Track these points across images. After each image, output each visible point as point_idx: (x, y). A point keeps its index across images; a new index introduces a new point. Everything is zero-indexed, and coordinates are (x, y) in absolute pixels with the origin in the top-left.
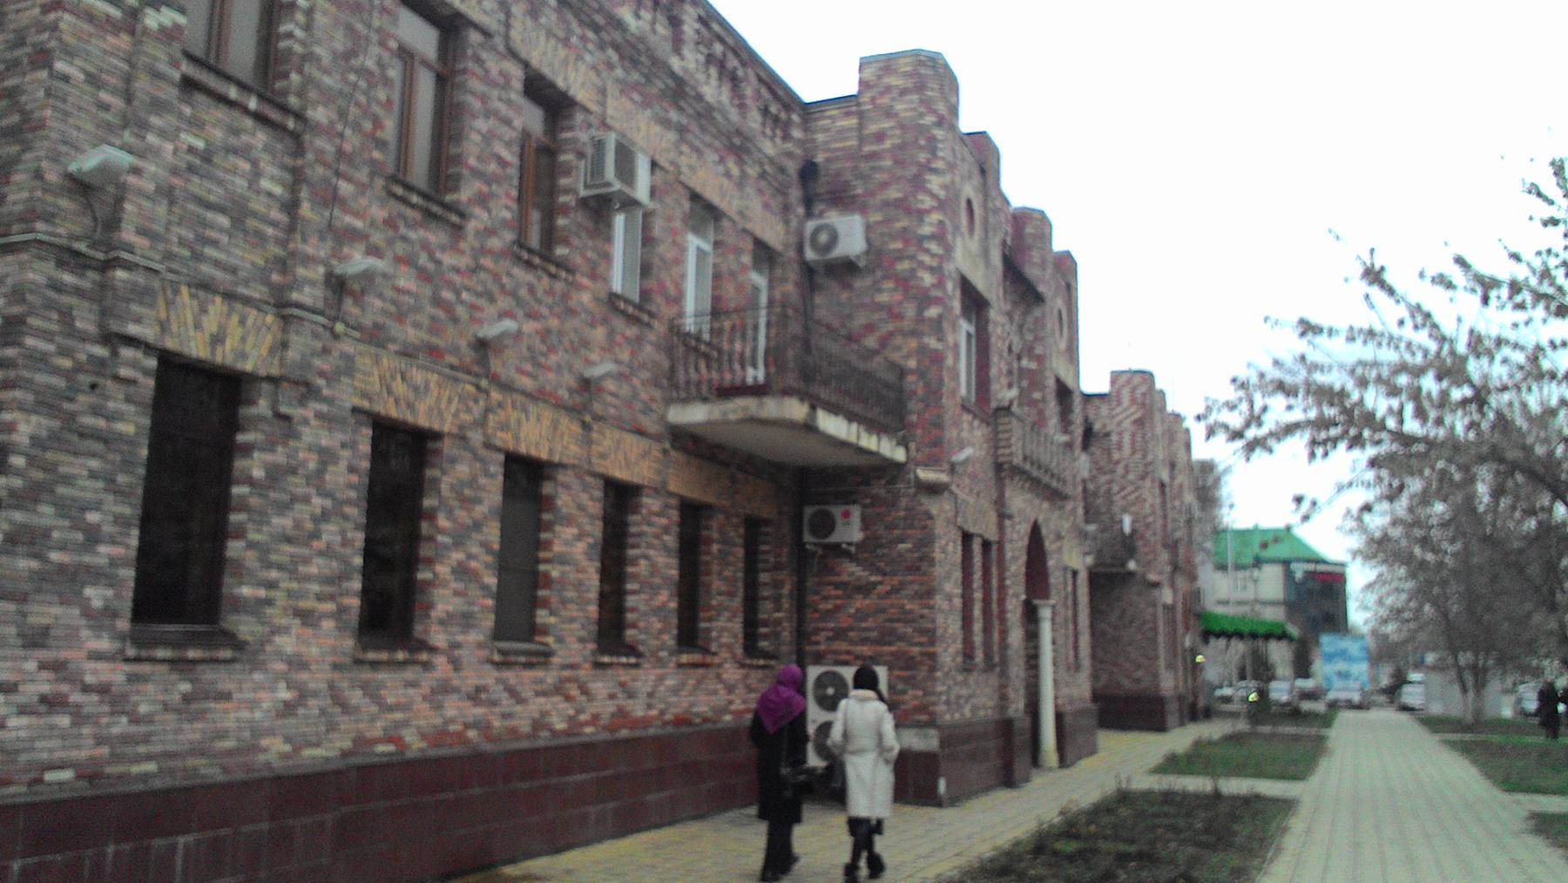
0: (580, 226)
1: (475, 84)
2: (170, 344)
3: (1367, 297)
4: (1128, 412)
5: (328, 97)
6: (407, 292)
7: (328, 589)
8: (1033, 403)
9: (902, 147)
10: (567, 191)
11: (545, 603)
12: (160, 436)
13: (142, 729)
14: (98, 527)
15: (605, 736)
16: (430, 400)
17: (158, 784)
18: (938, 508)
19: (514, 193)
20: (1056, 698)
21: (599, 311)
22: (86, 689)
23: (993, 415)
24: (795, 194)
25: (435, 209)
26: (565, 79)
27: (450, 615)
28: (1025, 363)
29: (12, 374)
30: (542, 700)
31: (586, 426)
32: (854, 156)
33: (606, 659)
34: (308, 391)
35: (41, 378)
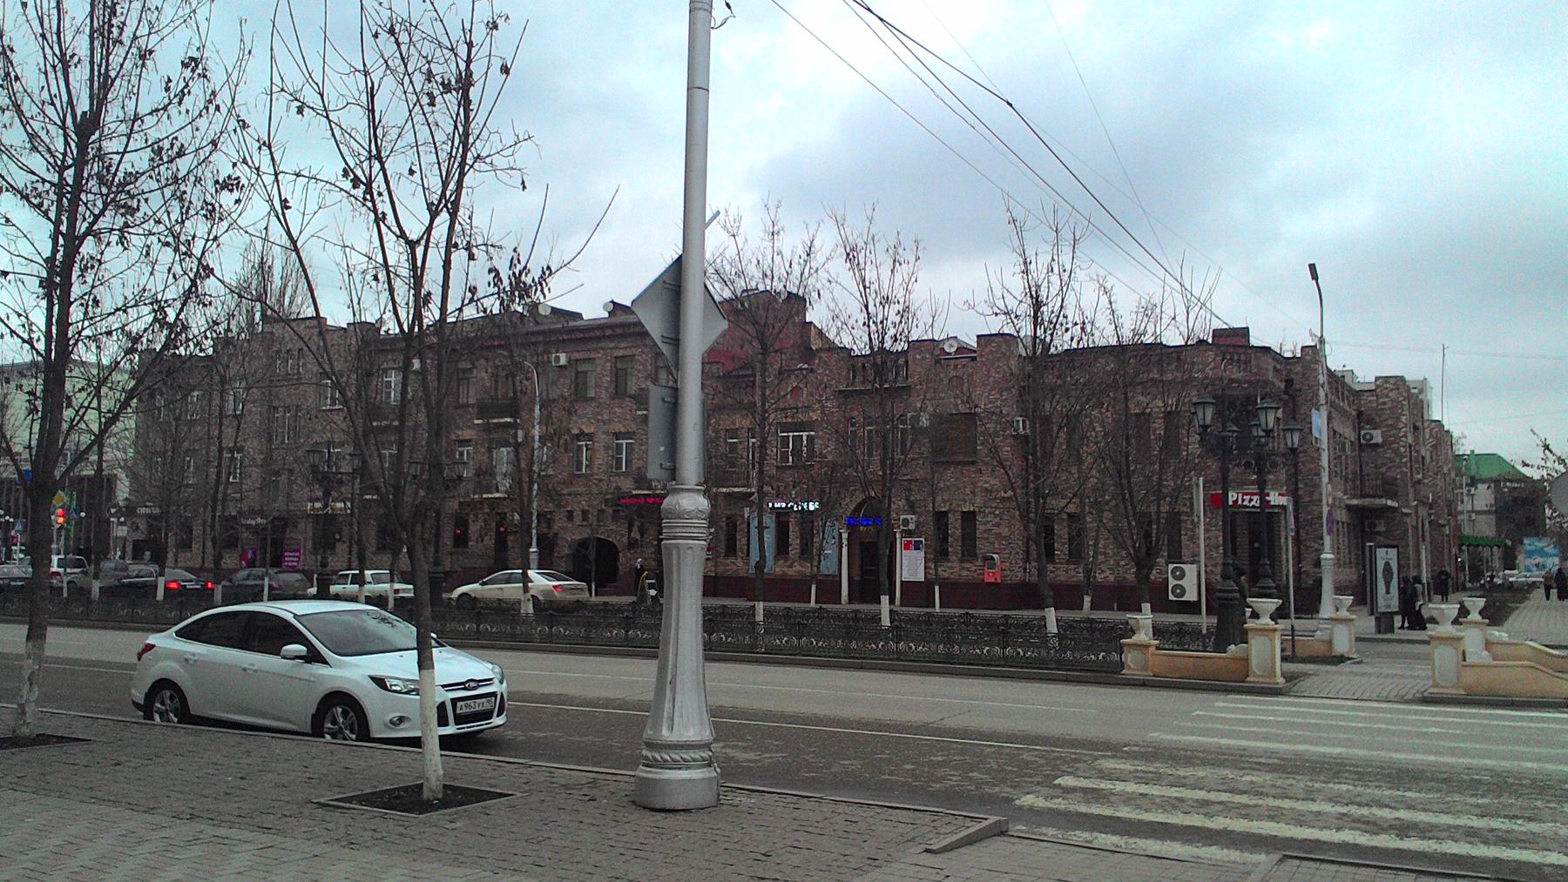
9: (1393, 407)
32: (1374, 409)
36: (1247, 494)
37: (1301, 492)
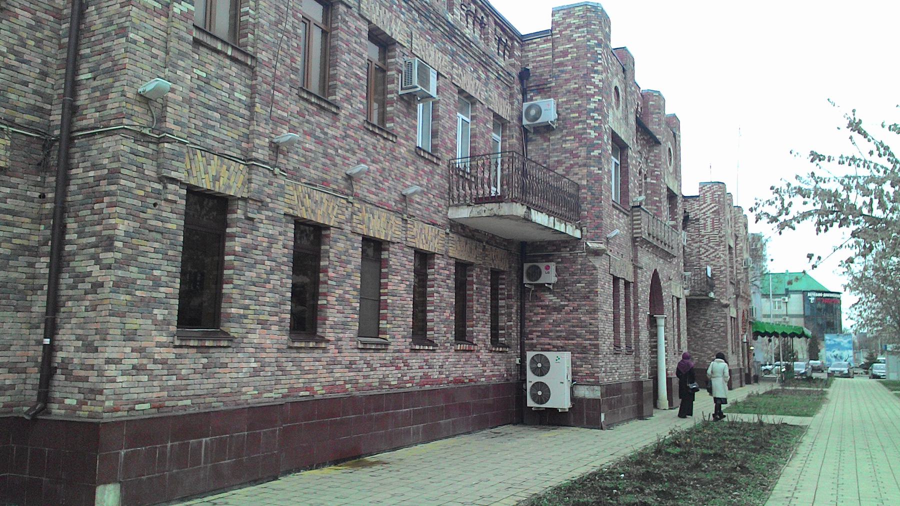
0: (399, 111)
1: (343, 35)
2: (193, 182)
3: (851, 138)
4: (711, 206)
5: (267, 46)
6: (311, 151)
7: (274, 309)
8: (654, 203)
9: (577, 59)
10: (391, 92)
11: (385, 317)
12: (188, 230)
13: (184, 382)
14: (159, 278)
15: (417, 388)
16: (323, 208)
17: (191, 411)
18: (600, 263)
19: (365, 95)
20: (667, 370)
21: (410, 158)
22: (155, 362)
23: (631, 211)
24: (517, 87)
25: (323, 104)
26: (390, 29)
27: (336, 323)
28: (649, 180)
29: (114, 199)
30: (384, 369)
31: (405, 221)
33: (417, 347)
34: (262, 205)
35: (128, 201)
37: (83, 98)
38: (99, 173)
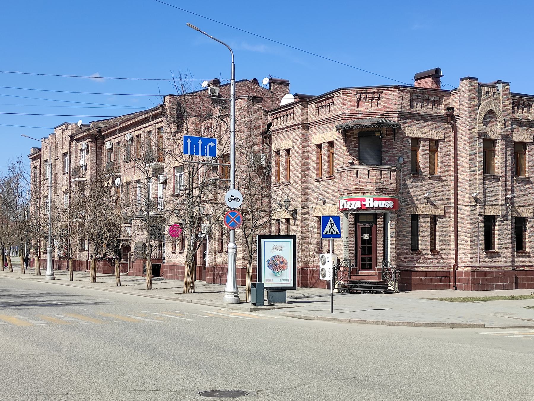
36: (349, 200)
38: (464, 215)
